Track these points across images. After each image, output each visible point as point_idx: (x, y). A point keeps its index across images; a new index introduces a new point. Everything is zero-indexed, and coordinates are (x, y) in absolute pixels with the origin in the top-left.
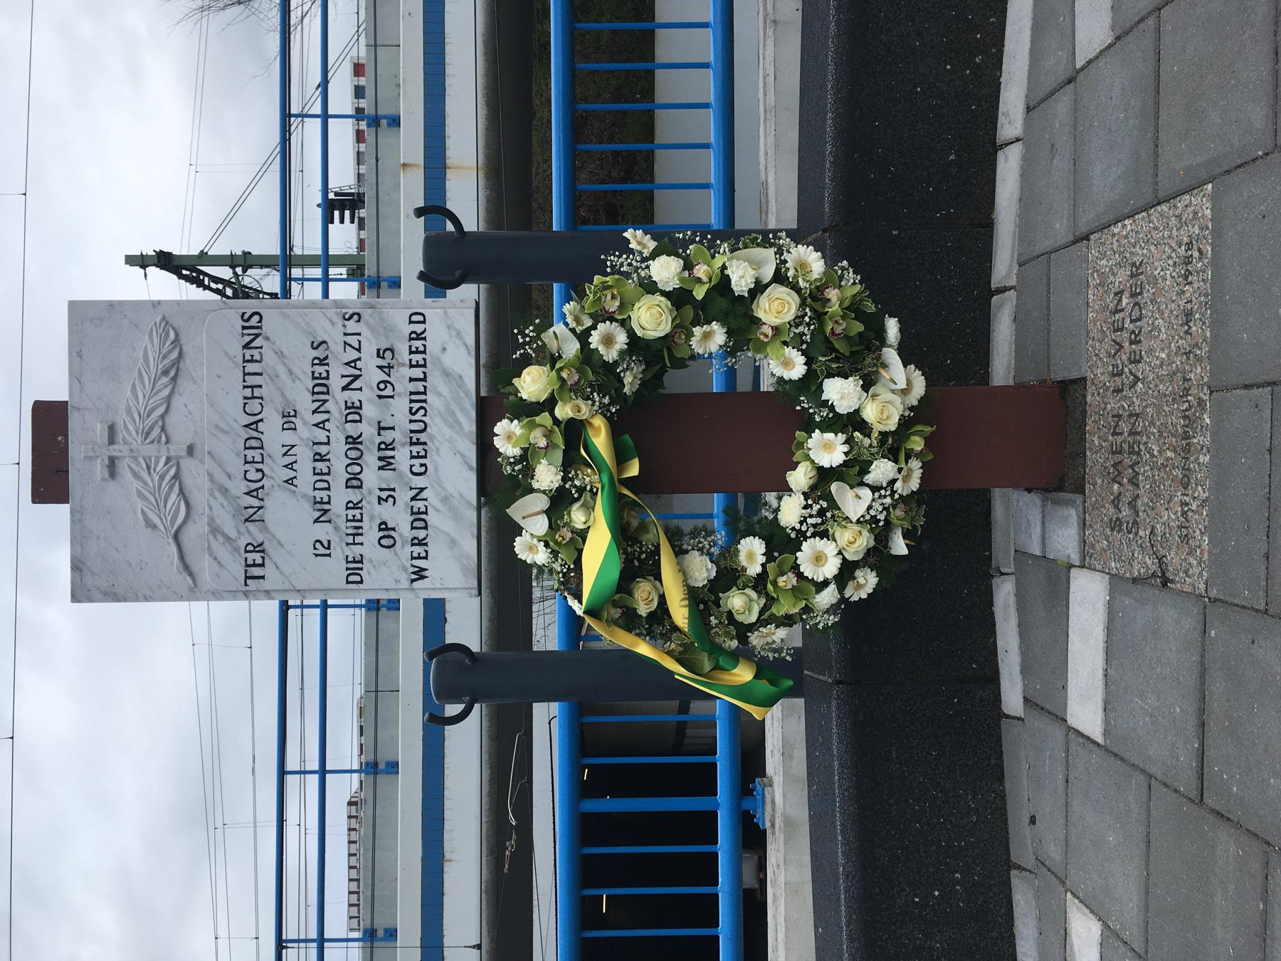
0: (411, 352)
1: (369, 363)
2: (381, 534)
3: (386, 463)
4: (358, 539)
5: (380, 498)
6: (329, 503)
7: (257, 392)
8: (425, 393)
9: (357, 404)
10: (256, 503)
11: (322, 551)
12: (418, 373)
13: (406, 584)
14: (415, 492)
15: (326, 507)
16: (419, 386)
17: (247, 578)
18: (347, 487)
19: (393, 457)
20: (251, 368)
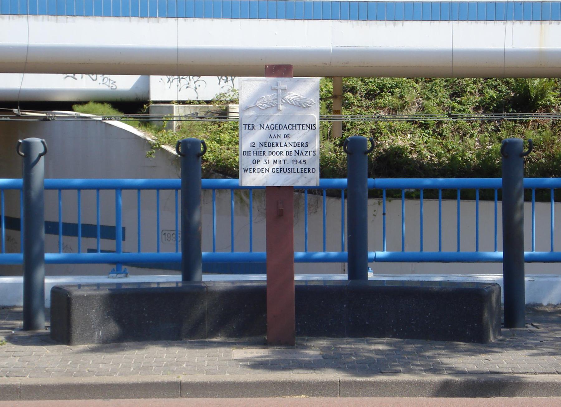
0: (305, 169)
1: (302, 158)
2: (257, 161)
3: (275, 162)
4: (255, 154)
5: (266, 160)
6: (265, 147)
7: (294, 128)
8: (294, 172)
9: (291, 154)
10: (265, 128)
11: (252, 145)
12: (299, 170)
13: (243, 167)
14: (268, 169)
15: (264, 146)
16: (296, 171)
17: (245, 125)
18: (269, 151)
19: (277, 164)
20: (301, 127)
